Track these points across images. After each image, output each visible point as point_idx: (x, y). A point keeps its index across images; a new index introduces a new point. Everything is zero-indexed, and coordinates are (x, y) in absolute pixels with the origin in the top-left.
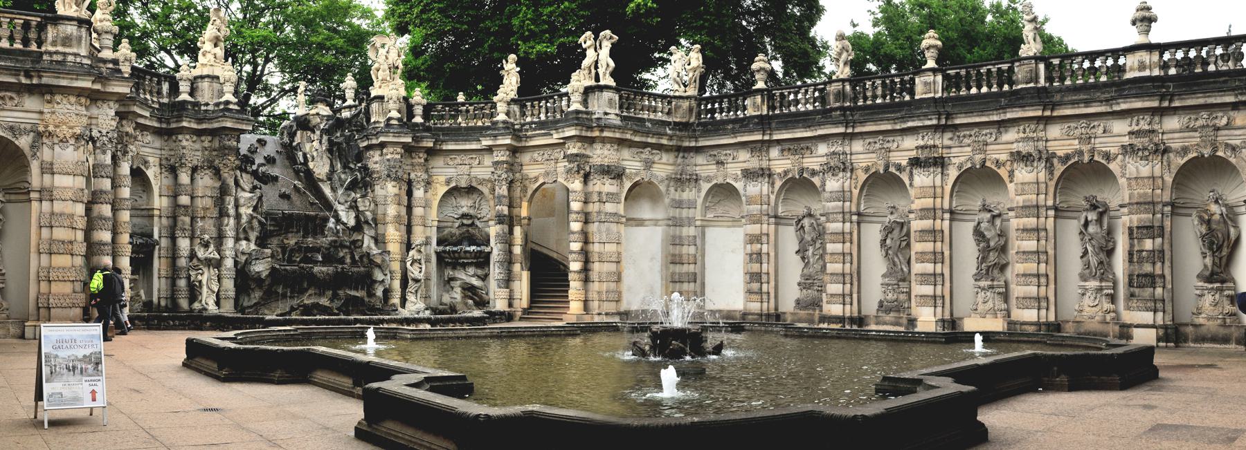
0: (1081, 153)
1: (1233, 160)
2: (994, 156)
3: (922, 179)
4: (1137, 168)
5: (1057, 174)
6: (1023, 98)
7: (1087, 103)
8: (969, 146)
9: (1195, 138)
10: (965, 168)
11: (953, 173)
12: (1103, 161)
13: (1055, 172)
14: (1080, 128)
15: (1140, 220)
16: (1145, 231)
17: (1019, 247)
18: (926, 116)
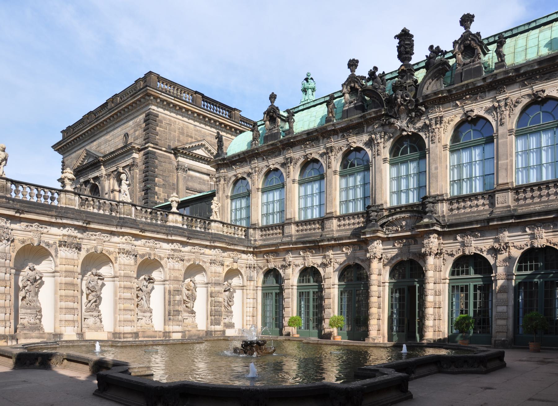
0: (150, 254)
1: (204, 267)
2: (107, 248)
3: (64, 253)
4: (174, 265)
5: (139, 262)
6: (127, 223)
7: (158, 233)
8: (95, 240)
9: (193, 256)
10: (90, 252)
11: (83, 254)
12: (159, 260)
13: (138, 261)
14: (151, 243)
15: (174, 287)
16: (176, 292)
17: (120, 296)
18: (77, 219)
